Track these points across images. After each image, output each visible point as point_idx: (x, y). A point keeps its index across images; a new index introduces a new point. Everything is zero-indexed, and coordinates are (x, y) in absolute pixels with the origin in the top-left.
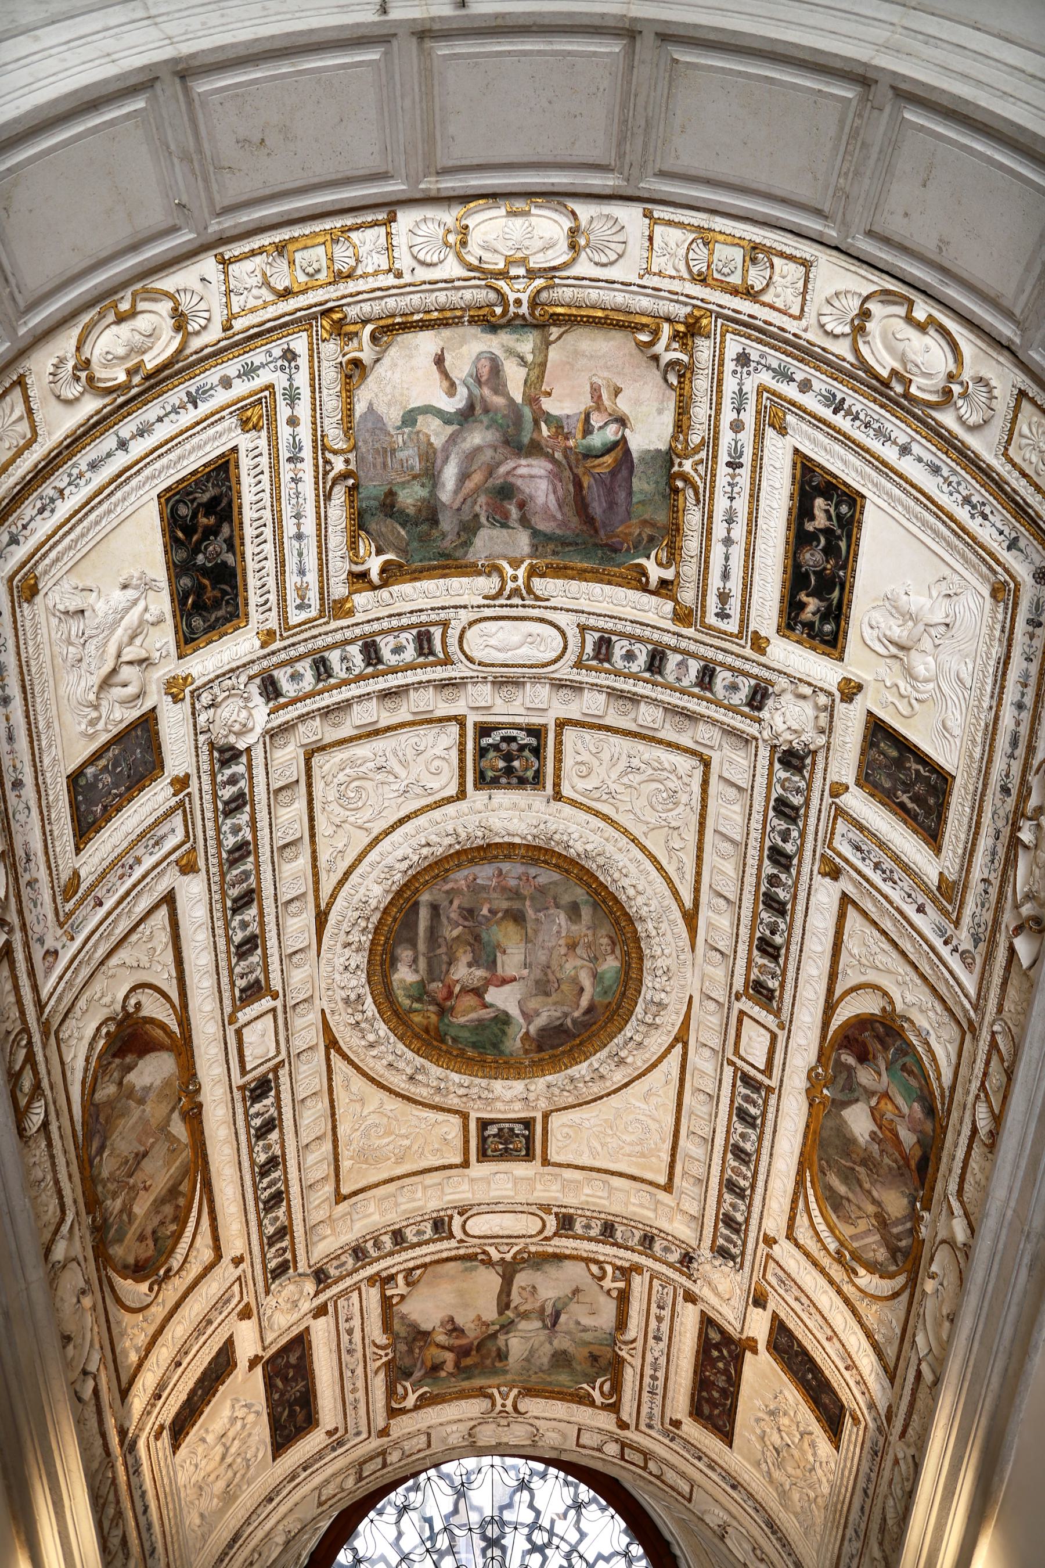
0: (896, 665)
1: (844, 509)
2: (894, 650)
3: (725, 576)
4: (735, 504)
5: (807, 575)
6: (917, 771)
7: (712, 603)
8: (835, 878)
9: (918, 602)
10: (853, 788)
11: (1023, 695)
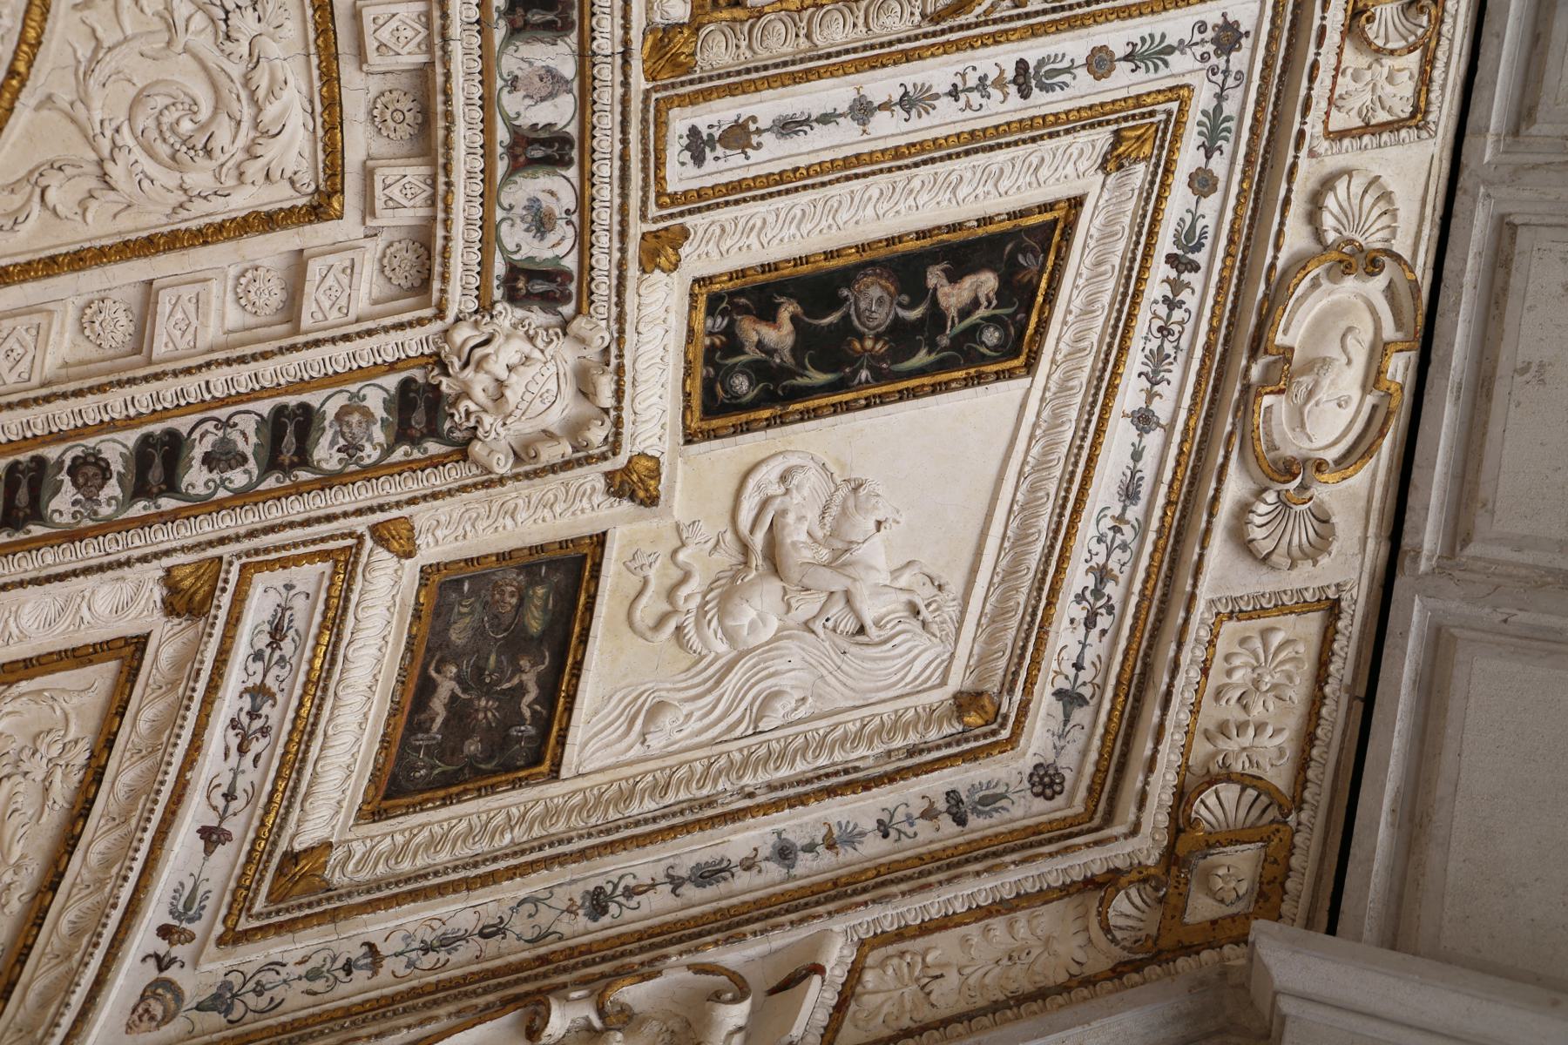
0: (728, 557)
1: (991, 336)
2: (758, 540)
3: (788, 127)
4: (944, 104)
5: (836, 303)
6: (521, 690)
7: (717, 114)
8: (170, 609)
9: (876, 554)
10: (412, 567)
11: (810, 848)
